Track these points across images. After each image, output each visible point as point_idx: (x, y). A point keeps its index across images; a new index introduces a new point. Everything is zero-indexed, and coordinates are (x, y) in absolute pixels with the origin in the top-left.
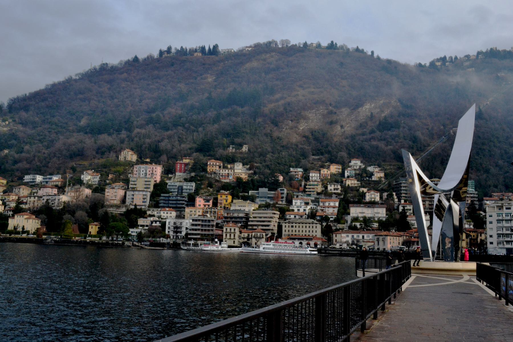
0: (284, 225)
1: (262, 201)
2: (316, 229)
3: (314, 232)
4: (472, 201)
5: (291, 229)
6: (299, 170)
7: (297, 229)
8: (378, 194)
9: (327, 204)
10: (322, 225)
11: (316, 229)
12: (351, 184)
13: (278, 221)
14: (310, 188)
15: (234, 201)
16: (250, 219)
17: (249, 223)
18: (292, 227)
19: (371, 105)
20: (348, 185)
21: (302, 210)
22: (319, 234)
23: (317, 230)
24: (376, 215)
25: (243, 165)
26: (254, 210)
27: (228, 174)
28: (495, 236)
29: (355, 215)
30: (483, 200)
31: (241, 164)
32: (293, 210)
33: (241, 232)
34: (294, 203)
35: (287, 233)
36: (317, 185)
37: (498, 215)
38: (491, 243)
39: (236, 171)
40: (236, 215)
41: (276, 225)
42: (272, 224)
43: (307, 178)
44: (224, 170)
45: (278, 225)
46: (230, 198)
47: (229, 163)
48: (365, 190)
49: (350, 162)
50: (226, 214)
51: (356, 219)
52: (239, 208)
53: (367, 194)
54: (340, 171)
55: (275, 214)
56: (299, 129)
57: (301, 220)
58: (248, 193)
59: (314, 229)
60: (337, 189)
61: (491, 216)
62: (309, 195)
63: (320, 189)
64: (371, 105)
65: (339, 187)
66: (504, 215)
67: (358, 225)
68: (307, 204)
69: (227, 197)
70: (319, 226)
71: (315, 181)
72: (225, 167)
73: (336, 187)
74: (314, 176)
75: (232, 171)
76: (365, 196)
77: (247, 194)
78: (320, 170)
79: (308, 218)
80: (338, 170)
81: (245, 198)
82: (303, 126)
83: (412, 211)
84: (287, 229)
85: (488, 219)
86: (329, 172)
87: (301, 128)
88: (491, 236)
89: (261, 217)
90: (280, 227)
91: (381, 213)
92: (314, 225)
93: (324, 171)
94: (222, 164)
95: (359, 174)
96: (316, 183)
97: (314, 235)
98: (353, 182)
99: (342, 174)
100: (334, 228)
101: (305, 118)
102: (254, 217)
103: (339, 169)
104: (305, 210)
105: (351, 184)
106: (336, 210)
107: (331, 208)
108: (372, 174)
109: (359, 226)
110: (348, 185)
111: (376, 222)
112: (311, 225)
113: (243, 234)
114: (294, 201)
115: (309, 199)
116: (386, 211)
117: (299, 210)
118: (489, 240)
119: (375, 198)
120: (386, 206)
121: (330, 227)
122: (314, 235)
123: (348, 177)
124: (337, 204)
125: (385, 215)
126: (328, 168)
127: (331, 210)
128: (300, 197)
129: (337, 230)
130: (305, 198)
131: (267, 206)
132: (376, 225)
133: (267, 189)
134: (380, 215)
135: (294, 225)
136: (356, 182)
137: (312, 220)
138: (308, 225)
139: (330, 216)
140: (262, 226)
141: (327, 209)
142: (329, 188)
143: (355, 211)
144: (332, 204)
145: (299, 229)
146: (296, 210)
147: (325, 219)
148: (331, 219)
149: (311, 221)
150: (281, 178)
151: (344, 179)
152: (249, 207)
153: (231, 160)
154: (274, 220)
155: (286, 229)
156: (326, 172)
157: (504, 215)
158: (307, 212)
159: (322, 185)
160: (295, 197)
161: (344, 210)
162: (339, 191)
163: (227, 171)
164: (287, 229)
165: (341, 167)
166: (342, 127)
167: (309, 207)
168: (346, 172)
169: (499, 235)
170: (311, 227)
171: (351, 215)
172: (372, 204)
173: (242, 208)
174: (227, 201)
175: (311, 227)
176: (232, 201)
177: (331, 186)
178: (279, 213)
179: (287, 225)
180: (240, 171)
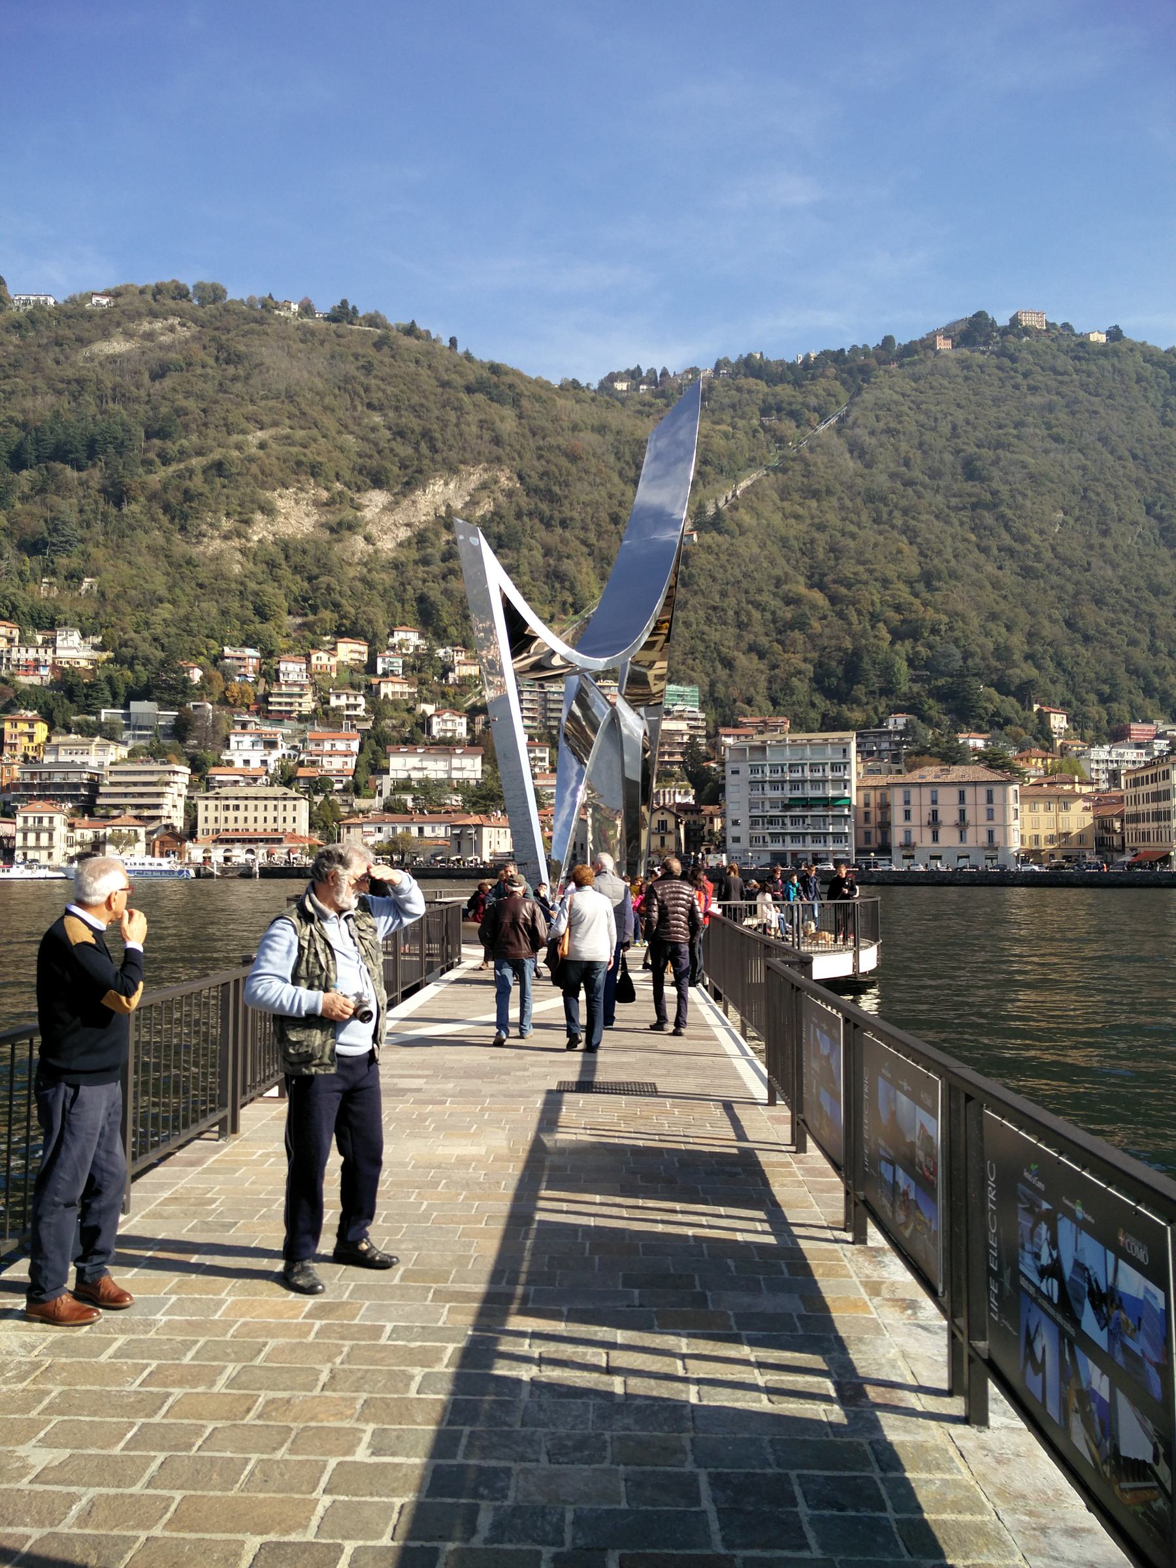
0: (201, 804)
1: (141, 737)
2: (294, 814)
3: (290, 820)
4: (692, 737)
5: (222, 814)
6: (249, 652)
7: (241, 814)
8: (464, 720)
9: (327, 746)
10: (311, 803)
11: (294, 814)
12: (394, 693)
13: (185, 792)
14: (280, 704)
15: (55, 740)
16: (102, 790)
17: (99, 801)
18: (227, 808)
19: (446, 484)
20: (386, 696)
21: (255, 763)
22: (303, 827)
23: (297, 816)
24: (456, 775)
25: (84, 636)
26: (112, 764)
27: (36, 660)
28: (745, 822)
29: (403, 775)
30: (717, 734)
31: (76, 636)
32: (230, 763)
33: (72, 826)
34: (233, 745)
35: (211, 825)
36: (301, 696)
37: (754, 770)
38: (737, 840)
39: (59, 653)
40: (57, 779)
41: (181, 803)
42: (167, 801)
43: (271, 675)
44: (23, 650)
45: (187, 805)
46: (41, 731)
47: (39, 627)
48: (430, 709)
49: (391, 634)
50: (27, 776)
51: (403, 786)
52: (69, 759)
53: (435, 720)
54: (365, 658)
55: (175, 773)
56: (248, 540)
57: (251, 791)
58: (97, 713)
59: (290, 814)
60: (355, 707)
61: (735, 772)
62: (279, 722)
63: (308, 704)
64: (446, 484)
65: (361, 700)
66: (767, 770)
67: (409, 799)
68: (271, 745)
69: (31, 726)
70: (303, 805)
71: (295, 684)
72: (24, 641)
73: (352, 701)
74: (291, 669)
75: (50, 651)
76: (430, 726)
77: (93, 718)
78: (308, 657)
79: (271, 785)
80: (356, 656)
81: (89, 731)
82: (260, 531)
83: (547, 764)
84: (211, 814)
85: (731, 780)
86: (333, 661)
87: (255, 538)
88: (735, 823)
89: (135, 784)
90: (191, 811)
91: (470, 768)
92: (289, 804)
93: (321, 659)
94: (16, 633)
95: (413, 668)
96: (296, 690)
97: (289, 830)
98: (398, 688)
99: (371, 667)
100: (344, 810)
101: (269, 511)
102: (112, 784)
103: (360, 653)
104: (264, 762)
105: (394, 693)
106: (351, 762)
107: (339, 756)
108: (447, 669)
109: (410, 804)
110: (386, 696)
111: (456, 791)
112: (281, 804)
113: (78, 832)
114: (233, 739)
115: (279, 732)
116: (483, 763)
117: (247, 762)
118: (732, 832)
119: (454, 731)
120: (481, 749)
121: (332, 805)
122: (289, 830)
123: (386, 674)
124: (355, 746)
125: (479, 775)
126: (333, 650)
127: (337, 763)
128: (251, 727)
129: (353, 813)
130: (268, 729)
131: (156, 753)
132: (456, 800)
133: (154, 705)
134: (466, 775)
135: (232, 803)
136: (406, 689)
137: (285, 789)
138: (271, 804)
139: (333, 779)
140: (138, 807)
141: (325, 760)
142: (334, 702)
143: (402, 765)
144: (341, 746)
145: (246, 814)
146: (239, 764)
147: (318, 786)
148: (338, 786)
149: (278, 790)
150: (196, 675)
151: (375, 681)
152: (100, 757)
153: (46, 622)
154: (174, 789)
155: (209, 813)
156: (325, 661)
157: (767, 770)
158: (272, 767)
159: (314, 694)
160: (238, 728)
161: (372, 764)
162: (360, 712)
163: (32, 654)
164: (211, 814)
165: (364, 649)
166: (368, 539)
167: (276, 754)
168: (379, 660)
169: (754, 821)
170: (280, 808)
171: (392, 774)
172: (446, 746)
173: (79, 759)
174: (31, 737)
175: (280, 808)
176: (49, 739)
177: (338, 697)
178: (189, 771)
179: (212, 804)
180: (74, 650)
